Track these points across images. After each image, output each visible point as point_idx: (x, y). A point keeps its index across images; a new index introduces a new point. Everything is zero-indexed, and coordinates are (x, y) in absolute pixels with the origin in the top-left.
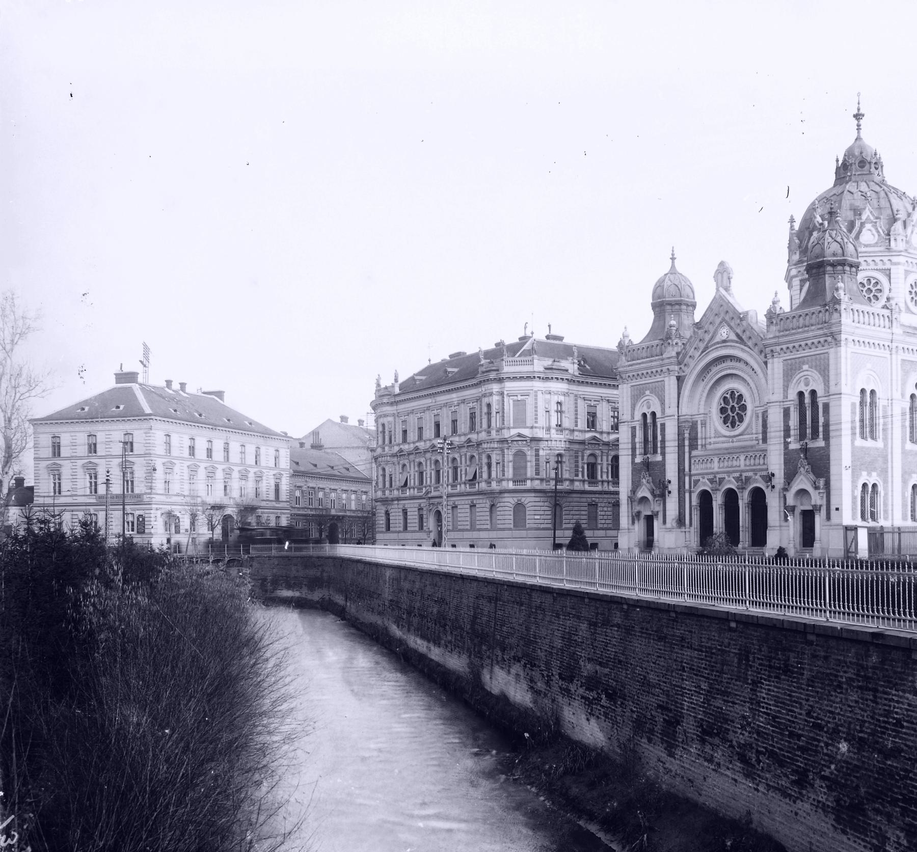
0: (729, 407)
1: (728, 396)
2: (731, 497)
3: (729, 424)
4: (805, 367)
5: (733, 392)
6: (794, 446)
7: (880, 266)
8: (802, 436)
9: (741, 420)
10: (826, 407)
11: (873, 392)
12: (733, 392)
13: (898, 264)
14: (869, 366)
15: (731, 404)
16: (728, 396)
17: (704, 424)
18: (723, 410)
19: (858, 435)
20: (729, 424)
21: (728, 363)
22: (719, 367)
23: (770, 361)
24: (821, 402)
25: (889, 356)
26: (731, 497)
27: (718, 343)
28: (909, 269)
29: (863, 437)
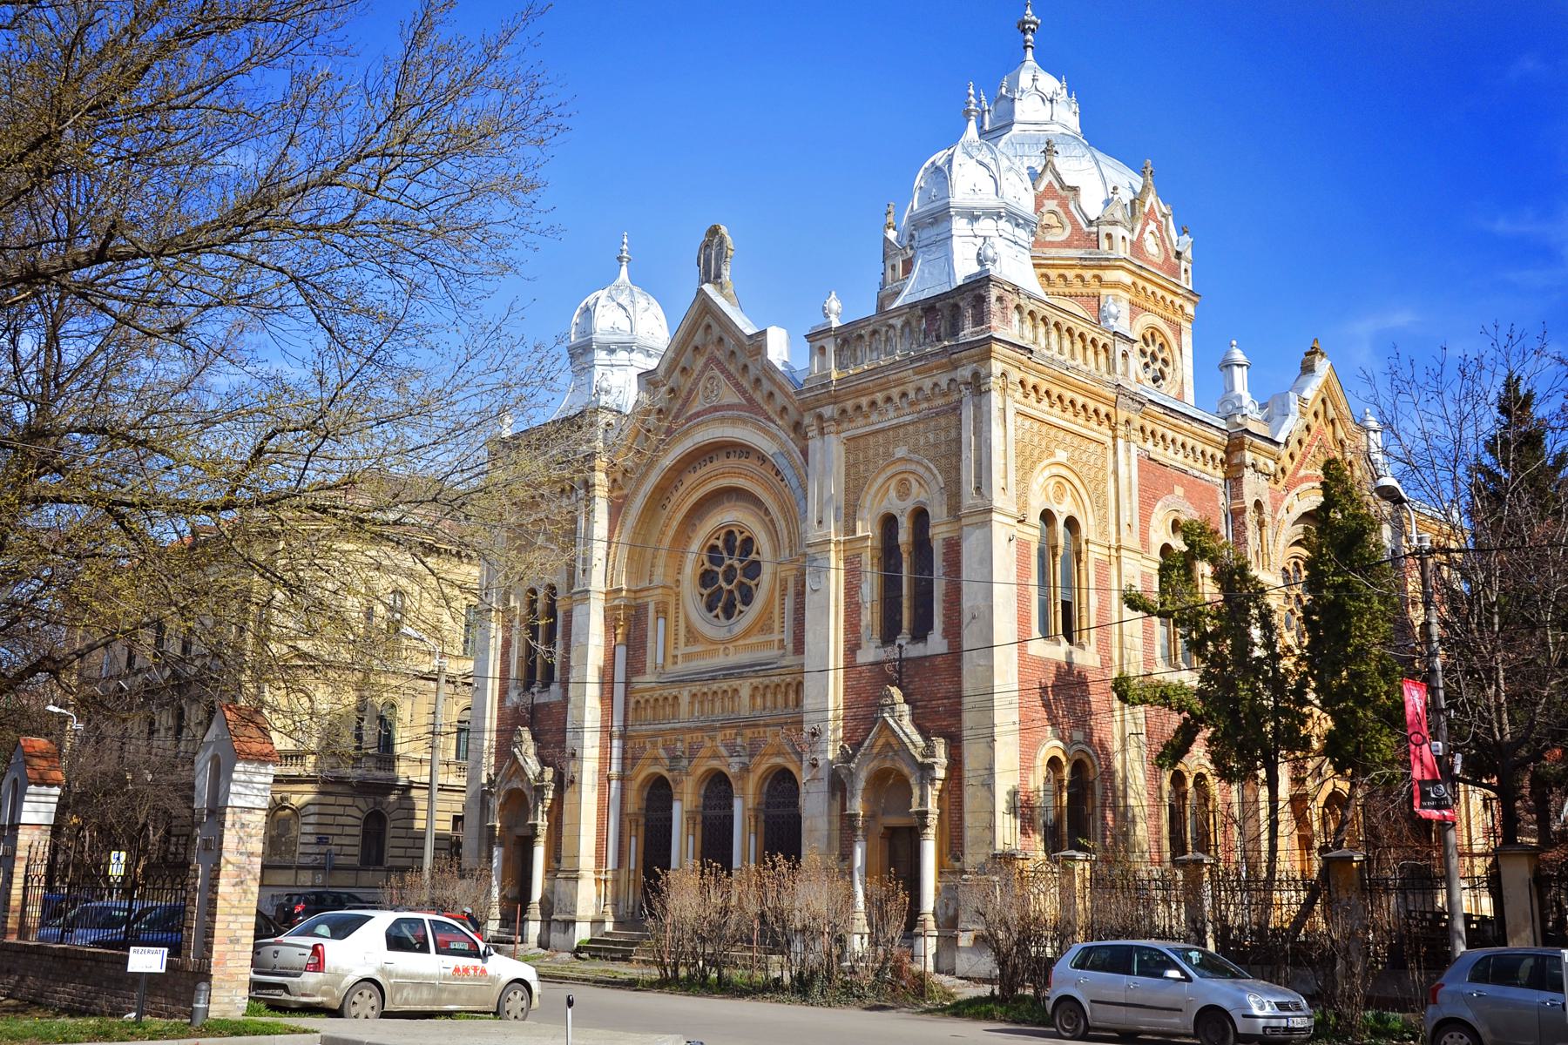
0: (720, 570)
1: (720, 543)
2: (718, 787)
3: (719, 611)
4: (901, 452)
5: (730, 533)
6: (869, 653)
7: (1078, 287)
8: (889, 633)
9: (747, 599)
11: (1071, 523)
12: (730, 533)
13: (1116, 285)
14: (1061, 456)
15: (728, 562)
16: (720, 543)
17: (662, 611)
18: (706, 578)
19: (1036, 632)
20: (719, 611)
21: (718, 464)
22: (700, 472)
23: (814, 444)
24: (939, 533)
25: (1110, 443)
26: (718, 787)
27: (697, 414)
28: (1140, 301)
29: (1046, 634)
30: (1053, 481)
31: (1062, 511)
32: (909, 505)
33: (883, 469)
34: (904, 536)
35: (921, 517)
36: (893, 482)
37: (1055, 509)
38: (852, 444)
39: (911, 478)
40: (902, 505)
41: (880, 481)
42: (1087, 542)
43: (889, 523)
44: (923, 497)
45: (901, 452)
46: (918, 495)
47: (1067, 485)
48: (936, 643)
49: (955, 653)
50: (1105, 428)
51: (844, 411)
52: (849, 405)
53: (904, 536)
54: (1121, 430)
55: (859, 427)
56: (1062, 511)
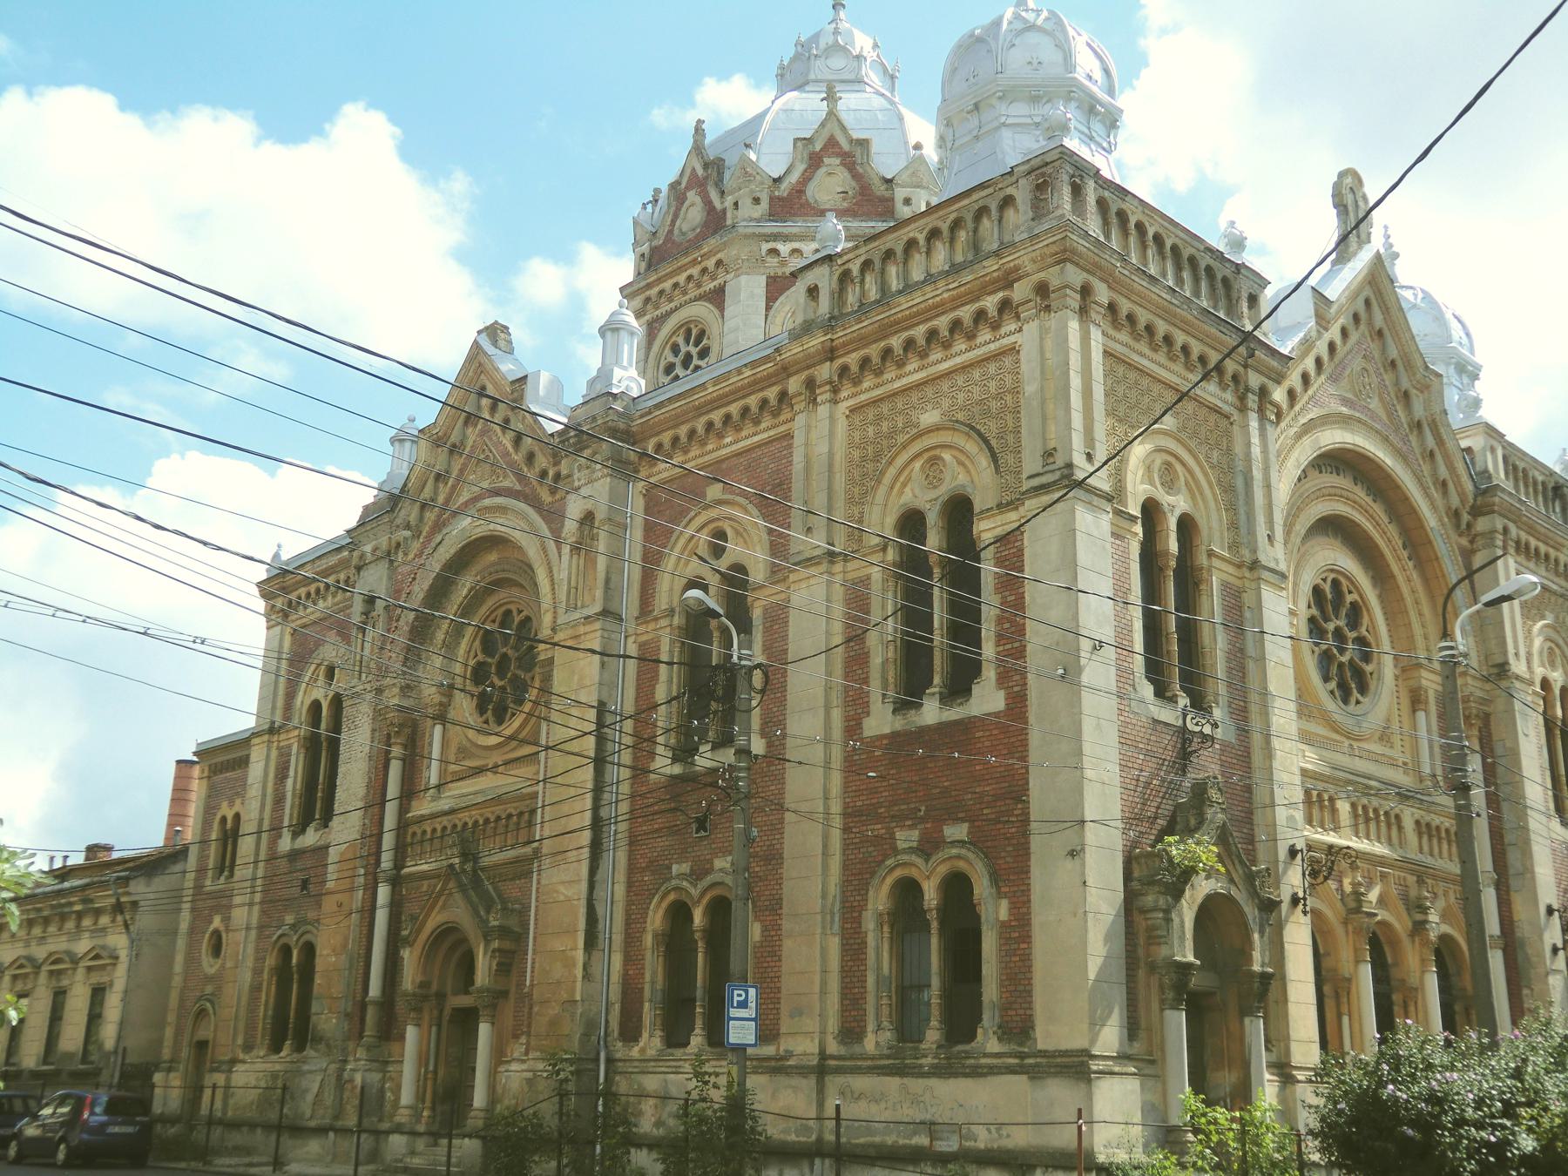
6: (881, 721)
8: (911, 690)
10: (1010, 542)
11: (1186, 526)
24: (986, 529)
31: (1176, 504)
32: (943, 491)
33: (904, 447)
34: (934, 543)
35: (959, 511)
36: (918, 465)
37: (1165, 499)
38: (857, 419)
39: (947, 456)
40: (932, 494)
41: (900, 461)
42: (1211, 554)
43: (912, 523)
44: (962, 478)
45: (929, 418)
46: (955, 478)
47: (1179, 467)
48: (987, 699)
49: (1017, 703)
50: (1229, 396)
51: (844, 370)
52: (852, 359)
53: (934, 543)
54: (1252, 401)
55: (870, 388)
56: (1176, 504)
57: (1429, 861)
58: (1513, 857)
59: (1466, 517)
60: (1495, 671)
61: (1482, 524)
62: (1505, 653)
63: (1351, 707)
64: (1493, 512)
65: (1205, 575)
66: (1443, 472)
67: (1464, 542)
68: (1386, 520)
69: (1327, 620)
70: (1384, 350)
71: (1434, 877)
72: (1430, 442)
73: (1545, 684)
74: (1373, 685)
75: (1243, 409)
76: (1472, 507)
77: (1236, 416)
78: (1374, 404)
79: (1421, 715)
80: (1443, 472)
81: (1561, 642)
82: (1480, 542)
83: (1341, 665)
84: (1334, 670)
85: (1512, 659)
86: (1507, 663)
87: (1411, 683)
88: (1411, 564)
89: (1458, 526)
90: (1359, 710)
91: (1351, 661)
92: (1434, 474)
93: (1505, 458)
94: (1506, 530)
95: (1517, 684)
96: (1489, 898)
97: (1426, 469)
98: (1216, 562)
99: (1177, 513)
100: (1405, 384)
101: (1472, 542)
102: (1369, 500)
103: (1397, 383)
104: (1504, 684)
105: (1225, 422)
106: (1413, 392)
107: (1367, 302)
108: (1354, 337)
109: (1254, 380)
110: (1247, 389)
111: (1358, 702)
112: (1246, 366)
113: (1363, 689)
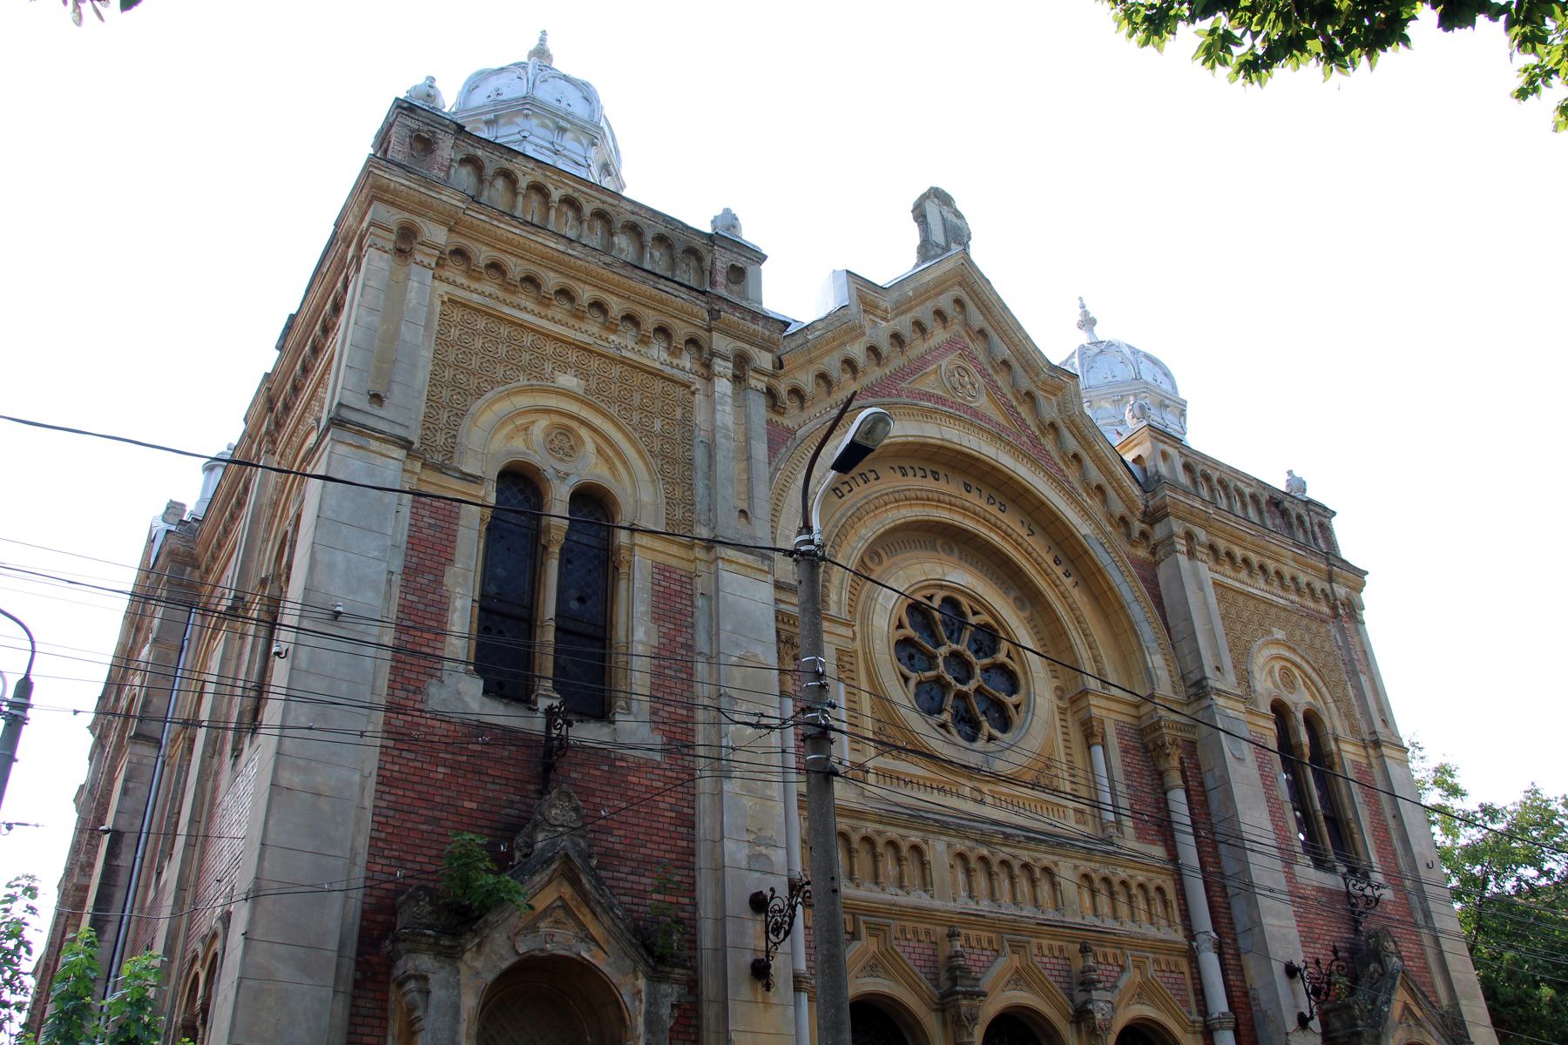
30: (543, 423)
50: (686, 361)
57: (1109, 923)
58: (1239, 909)
59: (1137, 526)
60: (1193, 690)
61: (1159, 532)
62: (1201, 667)
63: (980, 744)
64: (1167, 515)
65: (624, 554)
66: (1095, 476)
67: (1142, 553)
68: (1023, 532)
69: (938, 644)
70: (990, 352)
71: (1118, 945)
72: (1072, 444)
73: (1280, 710)
74: (1016, 720)
75: (709, 378)
76: (1145, 513)
77: (698, 384)
78: (982, 403)
79: (1098, 751)
80: (1095, 476)
81: (1298, 660)
82: (1161, 553)
83: (961, 696)
84: (950, 700)
85: (1209, 672)
86: (1204, 678)
87: (1082, 714)
88: (1068, 582)
89: (1128, 536)
90: (991, 747)
91: (978, 690)
92: (1084, 480)
93: (1187, 467)
94: (1189, 536)
95: (1220, 701)
96: (1210, 963)
97: (1072, 474)
98: (640, 539)
99: (573, 481)
100: (1025, 383)
101: (1153, 553)
102: (994, 509)
103: (1014, 385)
104: (1206, 702)
105: (680, 391)
106: (1039, 394)
107: (958, 302)
108: (939, 335)
109: (721, 343)
110: (713, 354)
111: (991, 738)
112: (710, 330)
113: (1005, 725)
